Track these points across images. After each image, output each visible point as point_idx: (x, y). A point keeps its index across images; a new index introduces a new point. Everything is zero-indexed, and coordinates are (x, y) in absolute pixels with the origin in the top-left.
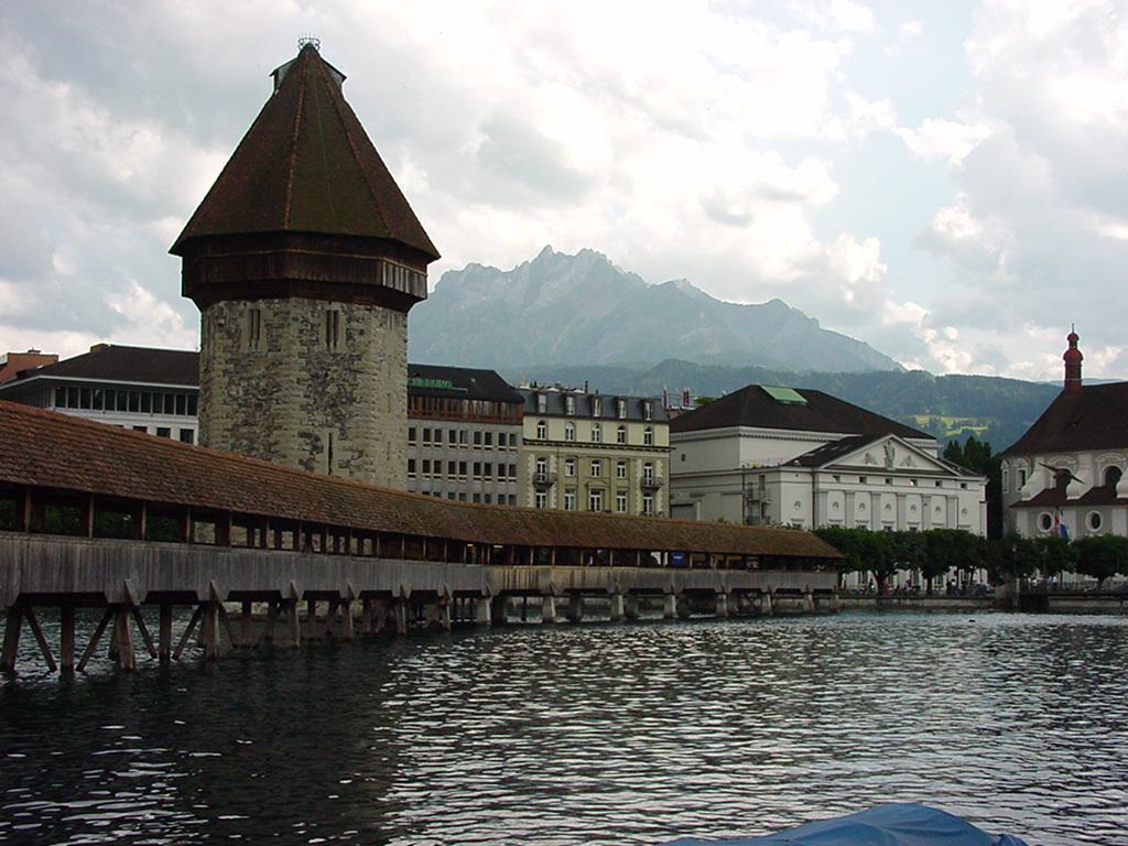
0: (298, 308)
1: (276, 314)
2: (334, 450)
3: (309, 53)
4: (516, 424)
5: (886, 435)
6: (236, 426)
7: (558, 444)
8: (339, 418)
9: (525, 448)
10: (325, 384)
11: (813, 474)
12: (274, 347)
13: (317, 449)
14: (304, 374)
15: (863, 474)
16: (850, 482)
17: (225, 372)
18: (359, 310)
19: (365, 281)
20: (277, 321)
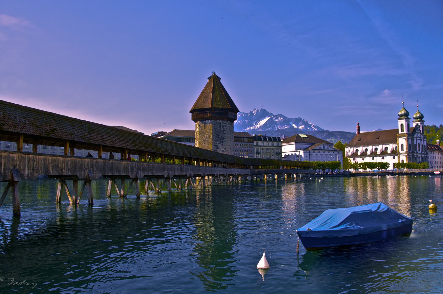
2: (221, 148)
4: (252, 143)
7: (260, 146)
9: (254, 147)
10: (219, 136)
13: (218, 148)
14: (215, 134)
16: (316, 152)
18: (225, 122)
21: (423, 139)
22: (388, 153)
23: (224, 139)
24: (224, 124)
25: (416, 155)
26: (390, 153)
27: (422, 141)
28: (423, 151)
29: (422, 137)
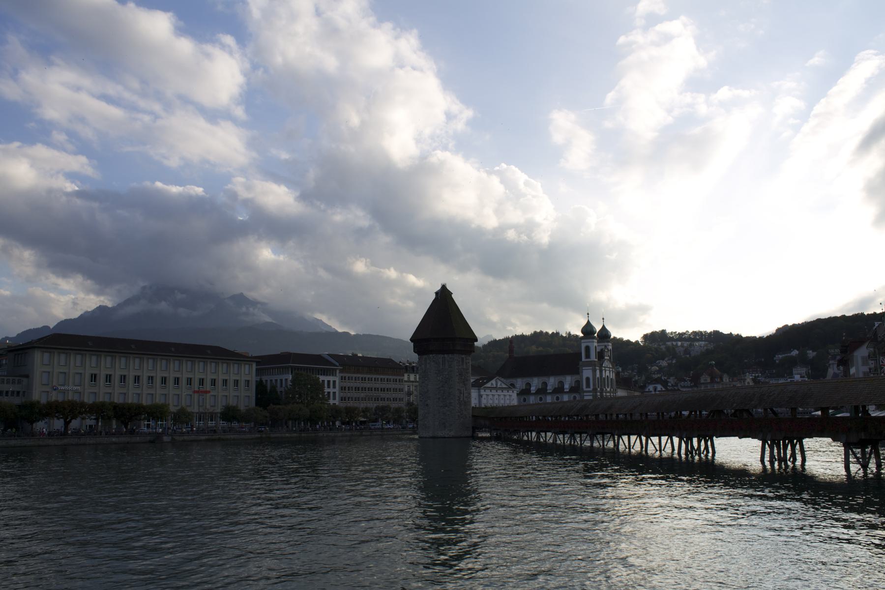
3: (444, 287)
5: (496, 377)
7: (413, 382)
10: (462, 376)
11: (479, 389)
15: (491, 389)
16: (488, 392)
17: (436, 373)
21: (611, 369)
22: (565, 390)
23: (467, 380)
25: (605, 394)
26: (568, 390)
27: (611, 372)
28: (612, 388)
29: (611, 366)
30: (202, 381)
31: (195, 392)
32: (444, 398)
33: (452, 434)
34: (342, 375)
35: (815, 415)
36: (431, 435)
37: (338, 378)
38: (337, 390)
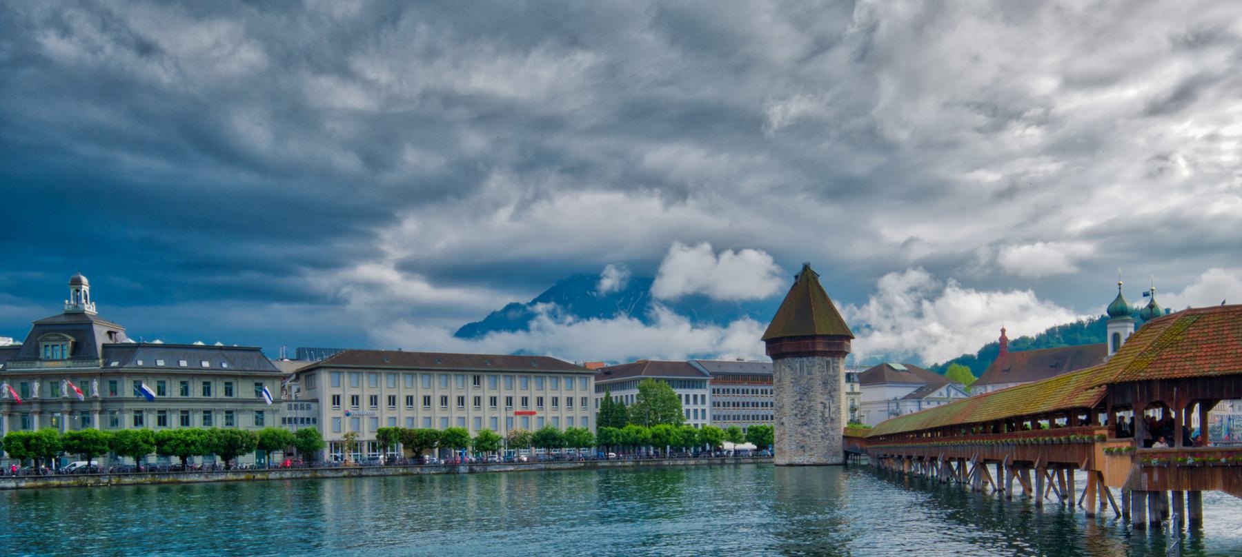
0: (817, 360)
1: (810, 362)
6: (797, 400)
8: (832, 396)
11: (919, 402)
12: (810, 373)
17: (791, 382)
19: (840, 350)
20: (811, 364)
23: (835, 390)
24: (836, 363)
30: (525, 401)
31: (517, 413)
32: (803, 413)
33: (814, 460)
34: (716, 387)
35: (1004, 428)
36: (787, 462)
37: (708, 391)
38: (707, 407)
